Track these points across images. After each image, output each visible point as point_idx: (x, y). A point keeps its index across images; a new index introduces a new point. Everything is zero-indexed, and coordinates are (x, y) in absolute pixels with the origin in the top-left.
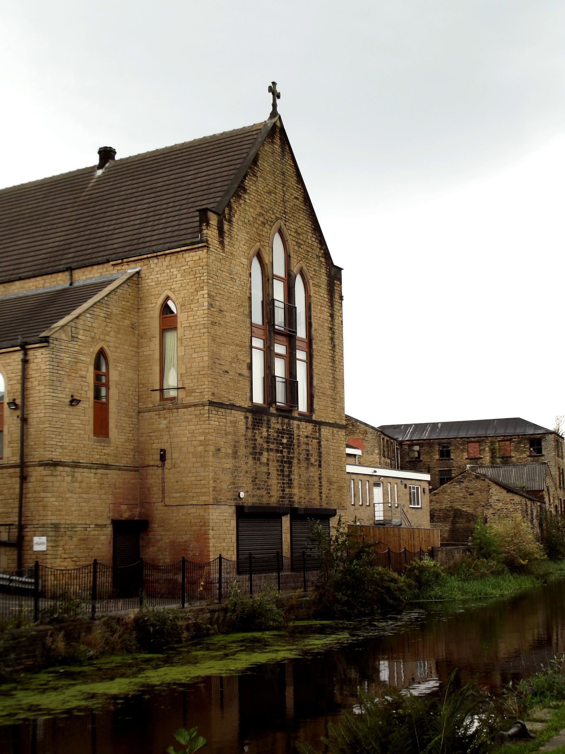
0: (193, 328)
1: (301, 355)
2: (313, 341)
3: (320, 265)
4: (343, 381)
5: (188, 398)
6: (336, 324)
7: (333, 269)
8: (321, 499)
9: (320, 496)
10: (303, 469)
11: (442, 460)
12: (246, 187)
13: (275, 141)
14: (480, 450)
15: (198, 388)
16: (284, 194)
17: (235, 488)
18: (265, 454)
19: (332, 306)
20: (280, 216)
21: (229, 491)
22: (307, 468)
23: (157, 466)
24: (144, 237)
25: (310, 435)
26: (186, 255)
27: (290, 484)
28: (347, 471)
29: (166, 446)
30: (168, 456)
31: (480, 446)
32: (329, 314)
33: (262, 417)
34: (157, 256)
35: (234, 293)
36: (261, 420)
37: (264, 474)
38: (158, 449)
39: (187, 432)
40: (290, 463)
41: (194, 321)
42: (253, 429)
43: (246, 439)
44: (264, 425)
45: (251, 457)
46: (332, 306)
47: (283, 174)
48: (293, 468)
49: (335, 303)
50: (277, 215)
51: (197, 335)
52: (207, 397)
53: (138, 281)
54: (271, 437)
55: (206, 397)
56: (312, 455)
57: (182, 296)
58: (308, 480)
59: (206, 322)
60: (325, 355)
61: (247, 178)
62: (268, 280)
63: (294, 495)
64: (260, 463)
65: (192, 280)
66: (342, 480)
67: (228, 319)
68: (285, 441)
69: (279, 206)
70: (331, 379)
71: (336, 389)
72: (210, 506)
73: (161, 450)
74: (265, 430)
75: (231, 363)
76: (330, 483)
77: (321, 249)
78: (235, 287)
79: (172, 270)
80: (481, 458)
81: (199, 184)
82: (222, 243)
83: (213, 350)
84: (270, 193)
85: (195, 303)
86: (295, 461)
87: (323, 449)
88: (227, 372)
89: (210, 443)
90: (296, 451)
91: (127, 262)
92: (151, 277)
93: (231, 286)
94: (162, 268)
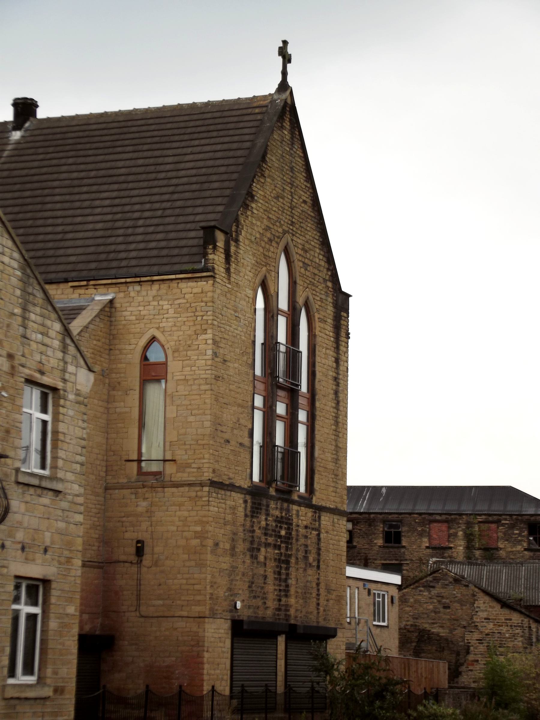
0: (190, 383)
1: (302, 416)
2: (317, 397)
3: (326, 292)
4: (346, 449)
5: (179, 474)
6: (341, 372)
7: (341, 297)
8: (318, 613)
10: (301, 571)
11: (387, 547)
12: (254, 193)
13: (284, 124)
14: (449, 536)
15: (194, 463)
16: (293, 197)
17: (231, 595)
18: (263, 550)
19: (337, 348)
20: (287, 229)
21: (225, 600)
22: (305, 570)
23: (131, 563)
24: (114, 251)
25: (309, 525)
26: (182, 285)
27: (286, 591)
28: (347, 575)
29: (145, 536)
30: (147, 550)
31: (449, 528)
32: (333, 359)
33: (261, 500)
34: (139, 282)
35: (238, 337)
36: (260, 504)
37: (261, 578)
38: (132, 540)
39: (177, 519)
40: (287, 562)
41: (192, 373)
42: (252, 517)
43: (244, 530)
44: (263, 511)
45: (248, 554)
46: (337, 348)
47: (292, 169)
48: (291, 569)
49: (341, 343)
50: (284, 227)
51: (195, 392)
52: (207, 475)
53: (111, 313)
54: (270, 527)
55: (206, 474)
56: (310, 553)
57: (175, 338)
59: (209, 376)
60: (327, 416)
61: (255, 180)
62: (273, 316)
63: (291, 606)
64: (258, 563)
65: (191, 319)
66: (341, 588)
67: (231, 372)
68: (283, 533)
69: (287, 214)
70: (333, 448)
71: (338, 462)
72: (207, 620)
73: (138, 542)
74: (263, 517)
75: (233, 429)
76: (329, 591)
77: (328, 269)
78: (240, 329)
79: (161, 303)
80: (451, 548)
81: (185, 180)
82: (228, 270)
83: (215, 413)
84: (277, 197)
85: (194, 350)
86: (293, 560)
87: (322, 544)
88: (228, 441)
89: (209, 535)
90: (294, 547)
91: (94, 285)
92: (129, 309)
93: (235, 327)
94: (146, 299)
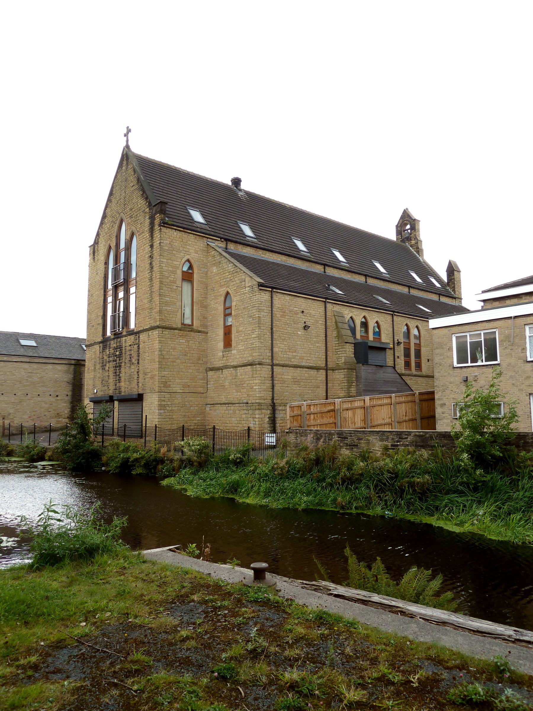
9: (138, 385)
10: (127, 368)
18: (108, 364)
22: (130, 367)
40: (120, 366)
58: (130, 375)
63: (122, 386)
74: (108, 350)
76: (145, 374)
86: (123, 364)
87: (141, 350)
90: (124, 358)
